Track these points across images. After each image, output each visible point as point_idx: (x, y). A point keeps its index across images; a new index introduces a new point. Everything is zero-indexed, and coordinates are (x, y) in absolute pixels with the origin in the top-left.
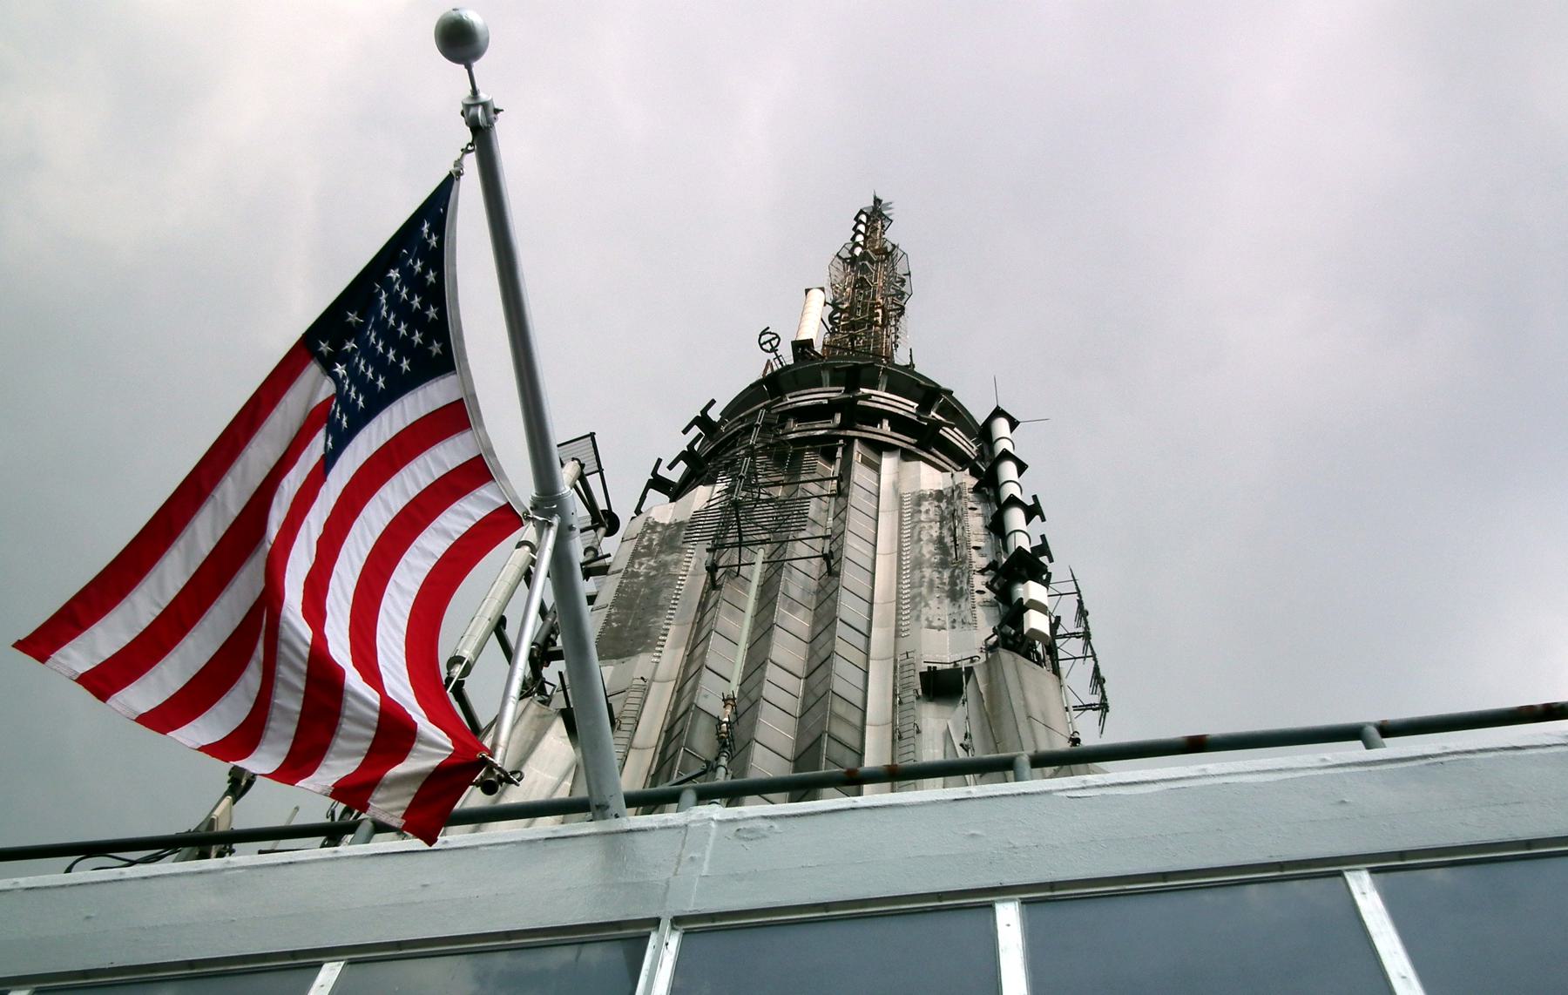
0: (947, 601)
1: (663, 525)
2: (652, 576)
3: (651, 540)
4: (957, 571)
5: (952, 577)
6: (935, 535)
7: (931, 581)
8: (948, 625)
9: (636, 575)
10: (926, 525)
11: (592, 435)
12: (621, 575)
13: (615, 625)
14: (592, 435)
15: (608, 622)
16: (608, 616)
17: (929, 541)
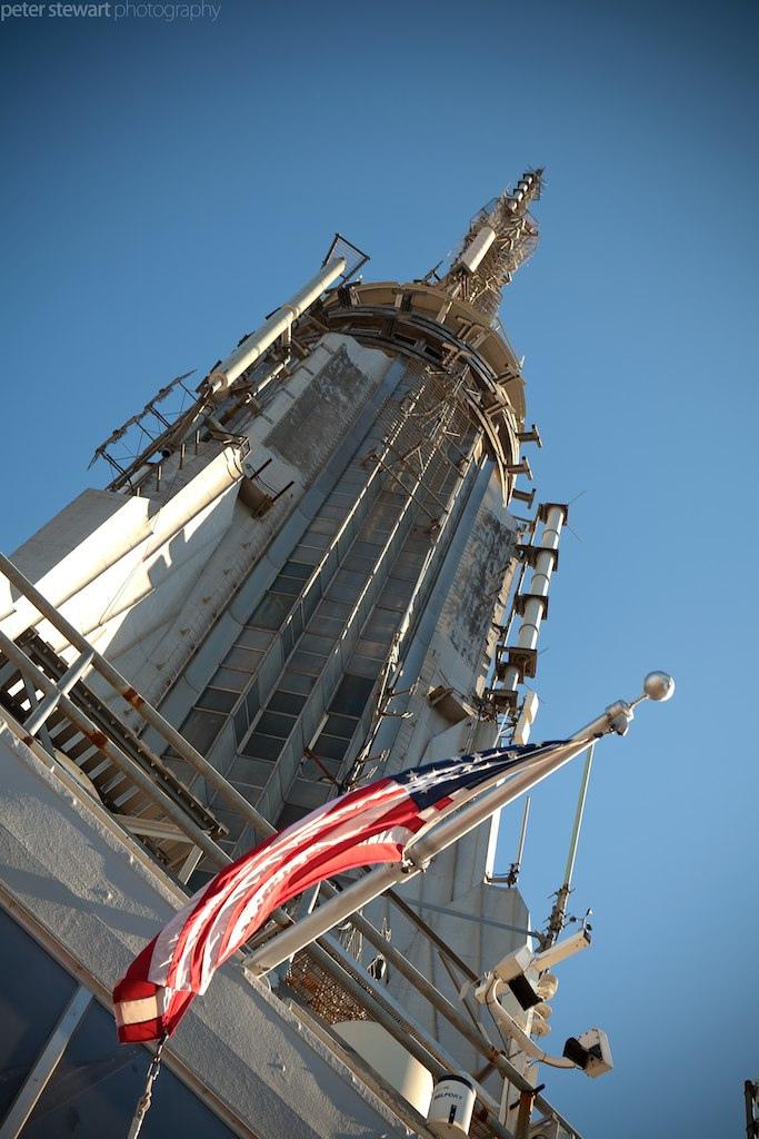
0: (468, 627)
1: (349, 360)
2: (327, 402)
3: (338, 366)
4: (482, 608)
5: (478, 608)
6: (484, 560)
7: (467, 600)
8: (460, 650)
9: (319, 390)
10: (483, 547)
11: (367, 258)
12: (312, 378)
13: (292, 422)
14: (367, 258)
15: (289, 414)
16: (292, 409)
17: (479, 562)
